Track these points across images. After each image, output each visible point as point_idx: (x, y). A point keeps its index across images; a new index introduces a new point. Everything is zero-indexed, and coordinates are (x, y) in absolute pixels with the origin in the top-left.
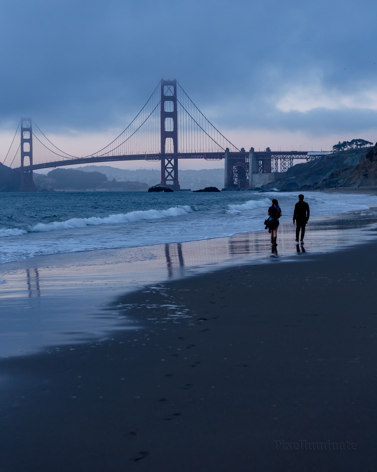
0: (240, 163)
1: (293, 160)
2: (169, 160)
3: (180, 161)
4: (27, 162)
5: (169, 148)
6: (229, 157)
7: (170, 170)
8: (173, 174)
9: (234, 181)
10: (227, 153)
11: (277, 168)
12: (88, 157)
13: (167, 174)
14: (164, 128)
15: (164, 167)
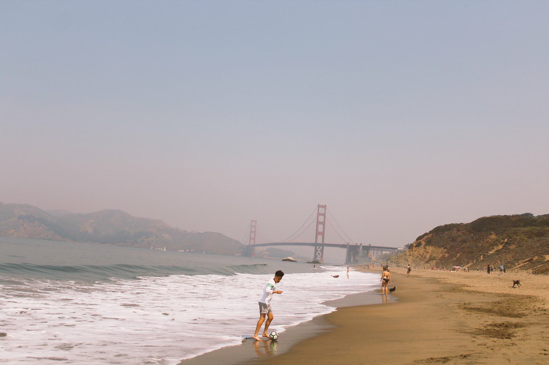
3: (325, 248)
4: (252, 243)
5: (320, 241)
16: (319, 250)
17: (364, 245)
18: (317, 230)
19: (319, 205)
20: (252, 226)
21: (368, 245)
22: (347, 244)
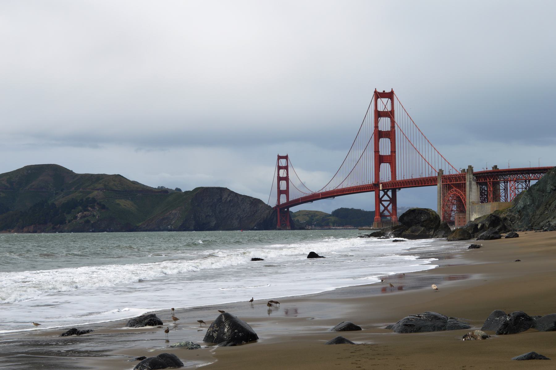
1: (529, 182)
2: (386, 191)
3: (399, 193)
4: (283, 200)
7: (386, 204)
8: (390, 208)
9: (451, 216)
11: (506, 195)
12: (319, 192)
13: (382, 208)
14: (379, 152)
15: (379, 200)
16: (386, 198)
17: (475, 170)
18: (377, 151)
19: (375, 92)
20: (280, 168)
21: (491, 169)
22: (437, 175)
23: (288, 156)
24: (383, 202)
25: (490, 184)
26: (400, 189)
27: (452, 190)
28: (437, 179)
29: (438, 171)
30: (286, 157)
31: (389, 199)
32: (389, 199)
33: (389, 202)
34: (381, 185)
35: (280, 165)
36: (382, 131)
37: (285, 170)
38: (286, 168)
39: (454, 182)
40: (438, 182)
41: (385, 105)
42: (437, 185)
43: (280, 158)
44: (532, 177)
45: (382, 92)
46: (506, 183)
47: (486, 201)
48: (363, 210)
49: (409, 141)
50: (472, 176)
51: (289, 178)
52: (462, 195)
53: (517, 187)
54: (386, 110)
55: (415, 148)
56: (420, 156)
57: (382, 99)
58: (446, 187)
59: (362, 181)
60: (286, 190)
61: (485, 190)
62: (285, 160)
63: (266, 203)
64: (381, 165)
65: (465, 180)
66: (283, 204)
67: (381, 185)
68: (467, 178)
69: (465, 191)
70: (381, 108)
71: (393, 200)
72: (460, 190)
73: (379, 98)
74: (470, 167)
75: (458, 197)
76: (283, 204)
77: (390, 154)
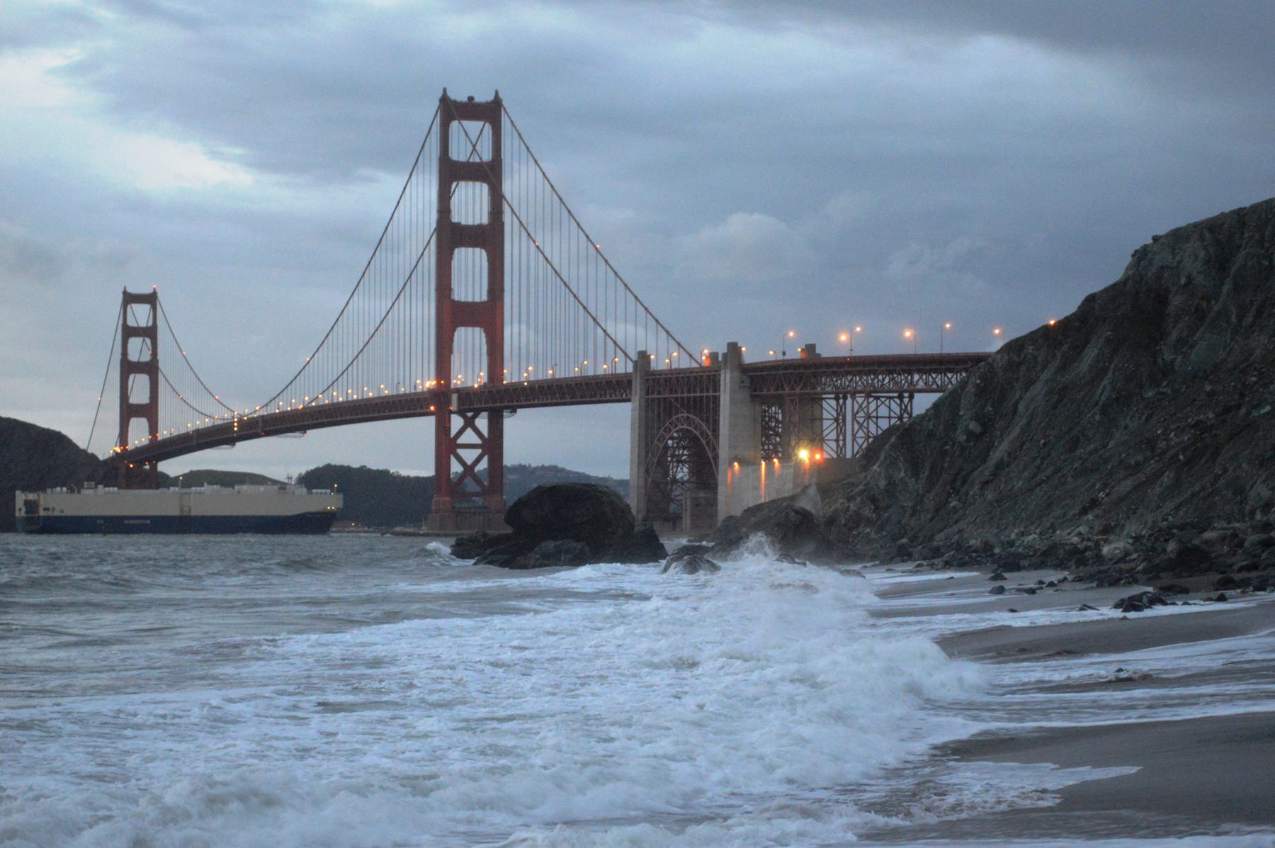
0: (685, 415)
1: (911, 397)
2: (469, 414)
4: (139, 436)
6: (648, 394)
7: (469, 456)
9: (672, 500)
10: (638, 373)
11: (841, 438)
13: (456, 468)
15: (446, 446)
16: (469, 437)
17: (750, 355)
20: (129, 332)
22: (630, 369)
23: (159, 295)
24: (460, 451)
25: (792, 401)
26: (515, 411)
27: (677, 419)
28: (630, 382)
29: (634, 356)
30: (151, 299)
31: (478, 441)
32: (476, 440)
33: (479, 451)
34: (455, 397)
35: (131, 322)
36: (463, 223)
37: (148, 341)
38: (150, 333)
39: (682, 393)
40: (633, 392)
41: (474, 142)
42: (629, 400)
43: (129, 299)
44: (921, 385)
45: (464, 99)
46: (841, 401)
47: (780, 455)
48: (397, 472)
49: (547, 259)
50: (737, 374)
51: (161, 365)
52: (708, 436)
53: (874, 414)
54: (477, 160)
55: (565, 284)
56: (581, 308)
57: (465, 123)
58: (659, 405)
59: (396, 382)
60: (146, 405)
61: (777, 421)
62: (146, 308)
63: (82, 445)
64: (456, 334)
65: (716, 388)
66: (139, 451)
67: (455, 397)
68: (722, 383)
69: (716, 423)
70: (459, 152)
71: (493, 445)
72: (701, 419)
73: (455, 119)
74: (734, 348)
75: (695, 440)
76: (136, 448)
77: (485, 298)
